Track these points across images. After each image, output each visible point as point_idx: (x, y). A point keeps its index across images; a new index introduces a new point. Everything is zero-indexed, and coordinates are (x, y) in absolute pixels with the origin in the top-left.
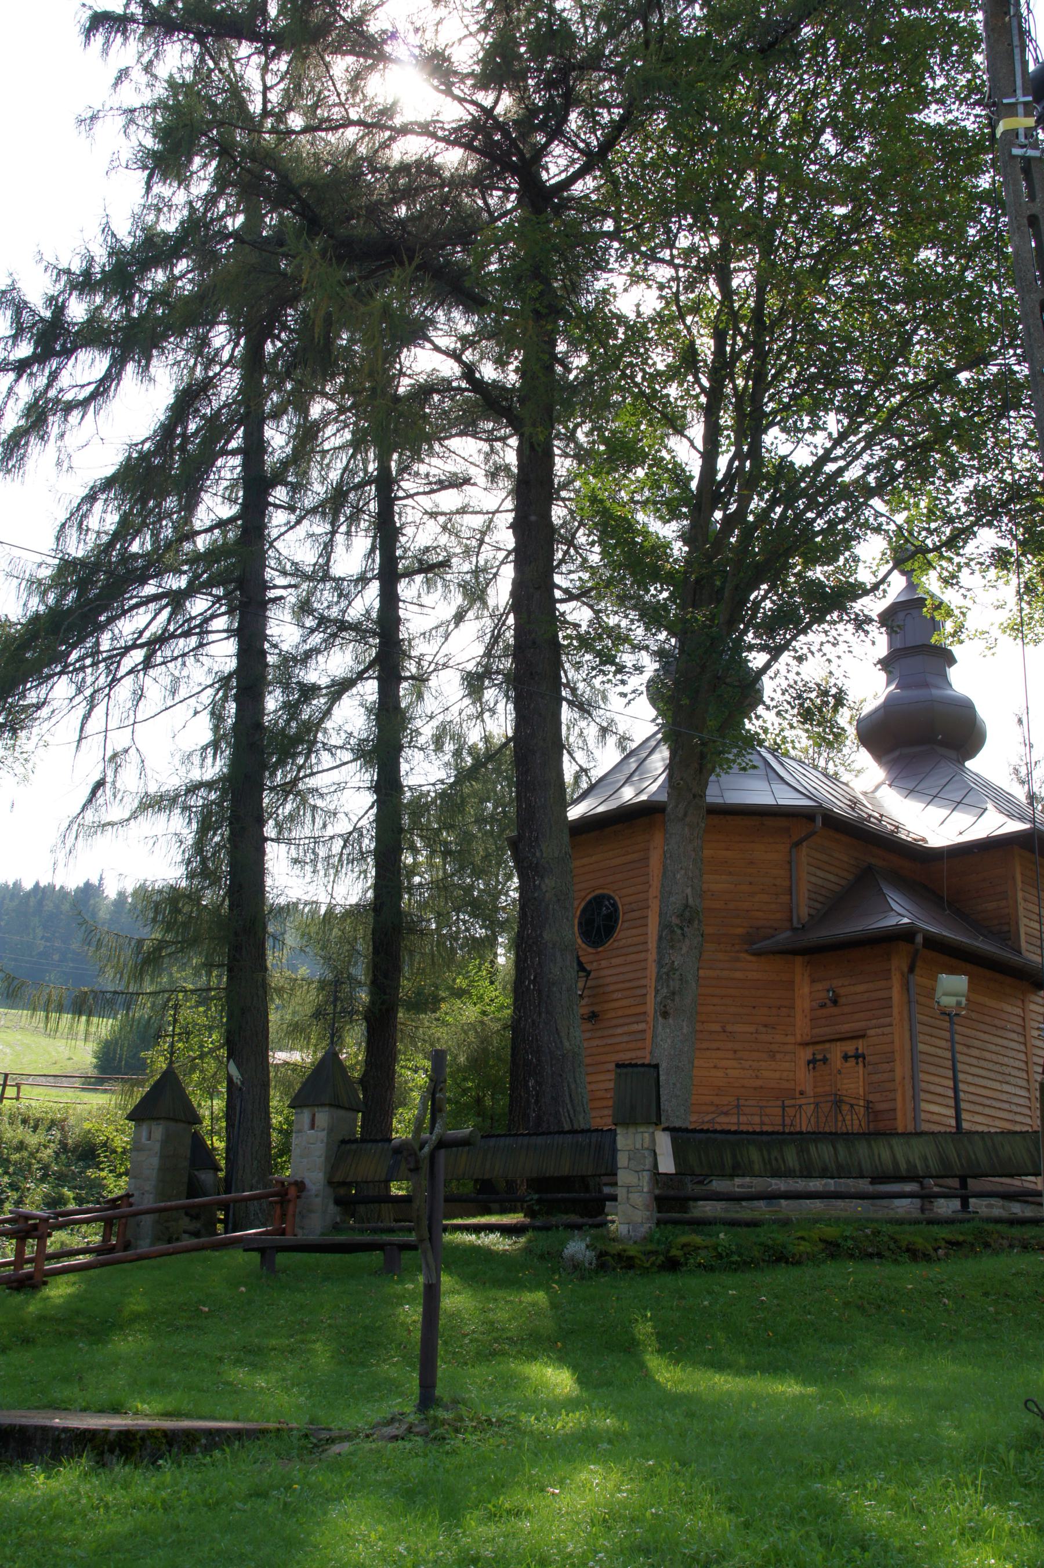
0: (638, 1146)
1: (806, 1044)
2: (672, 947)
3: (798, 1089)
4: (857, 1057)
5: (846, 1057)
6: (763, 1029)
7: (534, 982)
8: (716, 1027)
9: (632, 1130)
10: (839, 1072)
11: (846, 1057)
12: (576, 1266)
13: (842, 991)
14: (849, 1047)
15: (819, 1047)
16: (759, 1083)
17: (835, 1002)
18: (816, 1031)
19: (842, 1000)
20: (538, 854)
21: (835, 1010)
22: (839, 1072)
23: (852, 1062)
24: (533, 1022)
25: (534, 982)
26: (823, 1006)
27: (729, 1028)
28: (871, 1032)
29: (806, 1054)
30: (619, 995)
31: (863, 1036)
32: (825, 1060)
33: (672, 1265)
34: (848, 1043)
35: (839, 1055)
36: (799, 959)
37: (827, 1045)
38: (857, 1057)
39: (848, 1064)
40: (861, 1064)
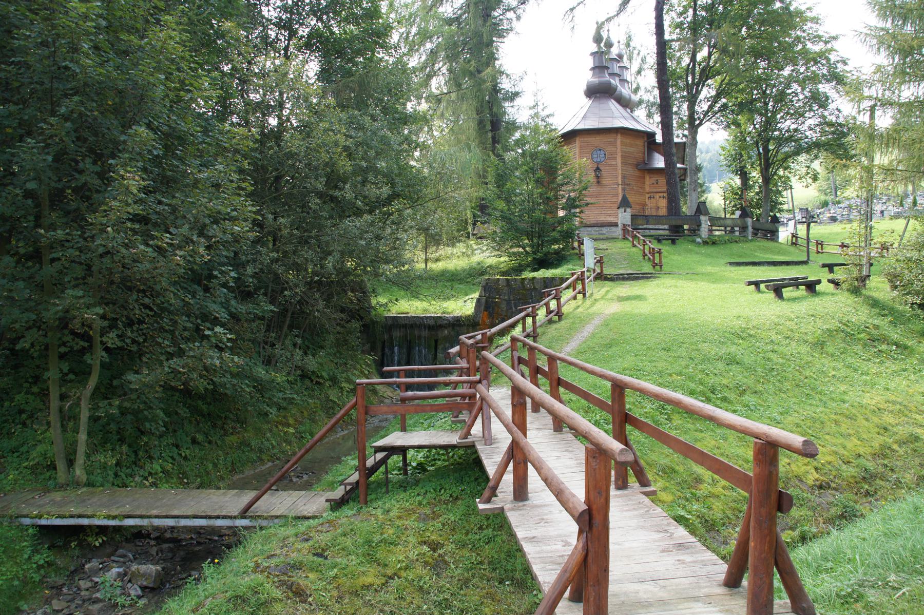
12: (699, 243)
29: (648, 195)
33: (714, 243)
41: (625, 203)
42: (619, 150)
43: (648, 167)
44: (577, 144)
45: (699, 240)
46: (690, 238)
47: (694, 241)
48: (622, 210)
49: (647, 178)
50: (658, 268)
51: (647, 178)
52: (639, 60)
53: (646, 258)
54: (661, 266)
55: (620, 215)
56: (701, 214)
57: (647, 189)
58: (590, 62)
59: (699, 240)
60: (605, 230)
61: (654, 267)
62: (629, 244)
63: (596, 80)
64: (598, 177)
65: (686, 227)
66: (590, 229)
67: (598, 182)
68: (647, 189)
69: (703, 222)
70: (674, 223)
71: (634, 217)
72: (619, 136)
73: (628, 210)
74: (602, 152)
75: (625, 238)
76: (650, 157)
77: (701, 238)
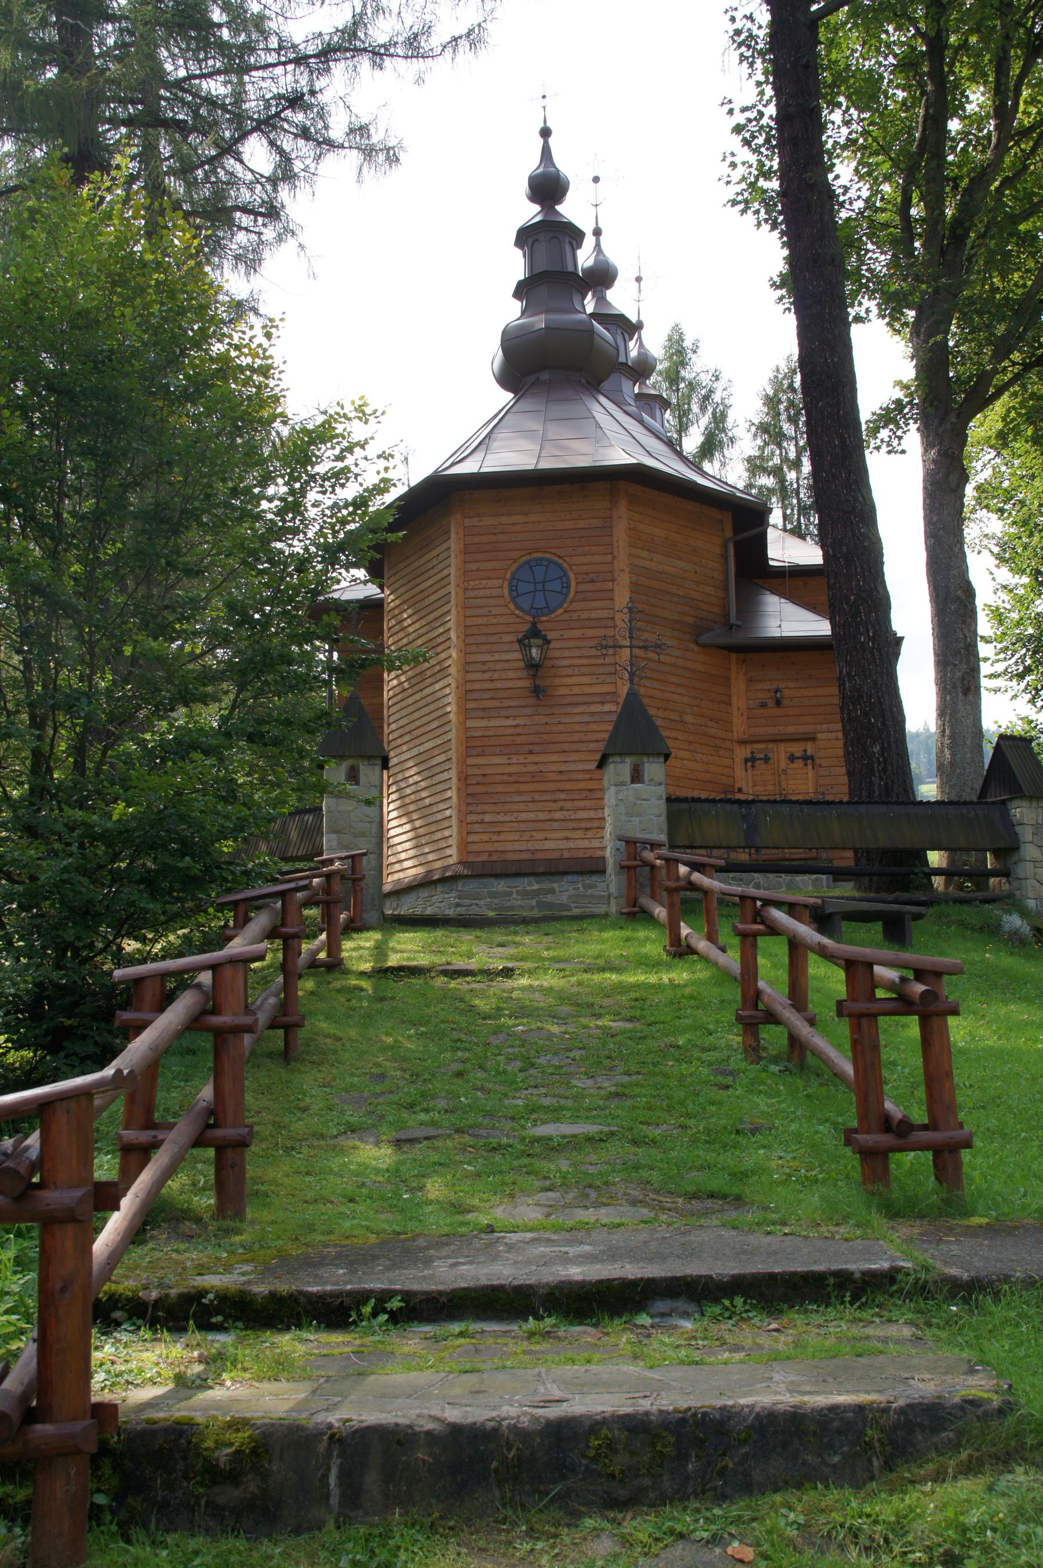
1: (743, 742)
2: (964, 622)
3: (737, 786)
4: (806, 758)
5: (792, 758)
6: (710, 723)
8: (675, 716)
9: (1035, 804)
11: (792, 758)
13: (786, 693)
14: (797, 749)
17: (778, 703)
18: (752, 730)
19: (785, 702)
21: (777, 711)
23: (799, 764)
24: (875, 682)
25: (873, 639)
26: (764, 705)
28: (819, 736)
29: (742, 753)
30: (569, 671)
31: (814, 739)
32: (766, 759)
34: (795, 744)
35: (783, 756)
36: (734, 656)
37: (771, 745)
38: (806, 758)
39: (795, 765)
40: (810, 767)
41: (634, 736)
42: (622, 562)
43: (738, 638)
44: (454, 543)
45: (1014, 921)
46: (966, 913)
47: (991, 931)
48: (620, 768)
49: (739, 685)
50: (911, 1165)
51: (739, 685)
52: (705, 421)
53: (772, 1037)
54: (947, 1157)
55: (610, 796)
56: (1017, 793)
57: (739, 726)
58: (515, 266)
59: (1014, 921)
60: (564, 891)
61: (875, 1162)
62: (652, 943)
63: (540, 322)
64: (533, 667)
65: (935, 858)
66: (501, 886)
67: (537, 691)
68: (739, 726)
69: (1026, 834)
70: (883, 837)
71: (678, 808)
72: (623, 508)
73: (654, 769)
75: (636, 914)
76: (749, 609)
77: (1024, 913)
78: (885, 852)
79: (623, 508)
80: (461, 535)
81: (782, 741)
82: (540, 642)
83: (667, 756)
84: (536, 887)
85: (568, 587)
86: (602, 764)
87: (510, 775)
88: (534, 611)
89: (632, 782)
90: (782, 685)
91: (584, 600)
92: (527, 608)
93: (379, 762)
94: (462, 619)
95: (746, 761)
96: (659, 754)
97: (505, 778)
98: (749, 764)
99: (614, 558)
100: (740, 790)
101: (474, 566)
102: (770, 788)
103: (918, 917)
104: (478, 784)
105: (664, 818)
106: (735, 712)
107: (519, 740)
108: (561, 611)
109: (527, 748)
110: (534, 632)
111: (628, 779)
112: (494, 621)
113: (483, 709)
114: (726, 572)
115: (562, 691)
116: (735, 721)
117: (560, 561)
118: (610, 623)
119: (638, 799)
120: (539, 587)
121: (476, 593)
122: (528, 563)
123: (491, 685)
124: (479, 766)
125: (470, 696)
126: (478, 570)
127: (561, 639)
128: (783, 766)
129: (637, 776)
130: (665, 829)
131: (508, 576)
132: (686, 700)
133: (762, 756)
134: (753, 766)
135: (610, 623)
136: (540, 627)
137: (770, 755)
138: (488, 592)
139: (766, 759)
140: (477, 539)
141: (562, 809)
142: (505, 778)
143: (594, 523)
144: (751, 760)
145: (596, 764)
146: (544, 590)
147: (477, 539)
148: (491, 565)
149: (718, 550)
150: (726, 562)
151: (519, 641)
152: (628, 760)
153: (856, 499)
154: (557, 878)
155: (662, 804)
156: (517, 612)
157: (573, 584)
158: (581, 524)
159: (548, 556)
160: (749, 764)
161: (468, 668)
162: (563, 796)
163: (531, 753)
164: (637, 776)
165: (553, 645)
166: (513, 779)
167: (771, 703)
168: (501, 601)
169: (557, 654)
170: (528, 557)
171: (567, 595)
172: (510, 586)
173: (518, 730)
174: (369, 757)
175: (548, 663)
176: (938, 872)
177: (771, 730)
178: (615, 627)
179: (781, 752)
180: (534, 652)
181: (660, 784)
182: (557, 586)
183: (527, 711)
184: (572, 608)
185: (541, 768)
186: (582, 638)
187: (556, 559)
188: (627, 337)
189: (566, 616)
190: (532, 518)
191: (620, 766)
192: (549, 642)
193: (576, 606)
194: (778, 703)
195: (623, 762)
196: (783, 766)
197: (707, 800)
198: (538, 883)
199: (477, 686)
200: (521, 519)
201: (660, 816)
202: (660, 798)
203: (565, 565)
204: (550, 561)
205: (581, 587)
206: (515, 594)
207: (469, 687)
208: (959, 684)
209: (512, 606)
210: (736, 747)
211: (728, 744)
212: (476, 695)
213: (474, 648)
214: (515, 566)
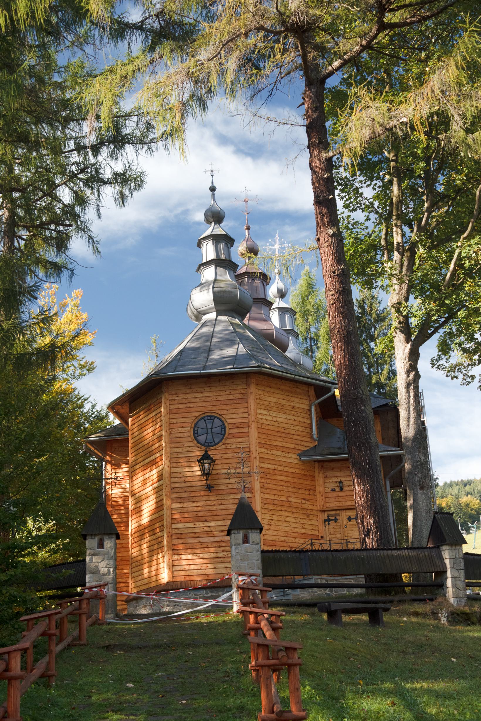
0: (457, 557)
1: (323, 511)
6: (304, 501)
7: (369, 464)
9: (454, 547)
10: (346, 526)
11: (350, 519)
13: (345, 483)
15: (333, 512)
16: (303, 531)
17: (341, 489)
18: (328, 505)
19: (345, 489)
20: (361, 392)
21: (341, 494)
22: (346, 526)
25: (369, 464)
26: (333, 490)
27: (290, 499)
32: (336, 520)
37: (338, 512)
39: (351, 523)
48: (238, 536)
49: (320, 478)
67: (209, 487)
68: (320, 503)
73: (253, 536)
74: (217, 422)
78: (379, 575)
79: (253, 388)
80: (168, 404)
81: (344, 510)
82: (209, 461)
83: (261, 530)
84: (210, 594)
85: (225, 431)
86: (229, 533)
87: (195, 533)
88: (206, 444)
89: (244, 543)
90: (343, 479)
91: (233, 438)
92: (203, 442)
93: (114, 536)
94: (168, 449)
95: (325, 521)
96: (256, 529)
97: (193, 535)
98: (327, 523)
99: (249, 415)
100: (322, 537)
101: (175, 421)
102: (338, 536)
103: (386, 610)
104: (178, 538)
105: (260, 561)
106: (318, 495)
107: (200, 514)
108: (221, 444)
109: (204, 518)
110: (206, 456)
111: (241, 542)
112: (186, 450)
113: (181, 498)
114: (311, 419)
115: (223, 487)
116: (318, 499)
117: (220, 417)
118: (248, 450)
119: (247, 552)
120: (209, 431)
121: (176, 435)
122: (203, 418)
123: (183, 485)
124: (178, 529)
125: (173, 491)
126: (177, 423)
127: (221, 459)
128: (345, 523)
129: (246, 540)
130: (261, 567)
131: (193, 425)
132: (290, 489)
133: (333, 518)
134: (329, 524)
135: (248, 450)
136: (210, 453)
137: (338, 518)
138: (182, 435)
139: (336, 520)
140: (176, 406)
141: (223, 551)
142: (193, 535)
143: (237, 396)
144: (328, 520)
145: (226, 533)
146: (212, 433)
147: (176, 406)
148: (182, 420)
149: (306, 407)
150: (311, 414)
151: (199, 461)
152: (241, 532)
153: (358, 392)
154: (221, 589)
155: (259, 553)
156: (198, 445)
157: (227, 429)
158: (231, 397)
159: (213, 414)
160: (327, 523)
161: (172, 476)
162: (224, 544)
163: (206, 521)
164: (246, 540)
165: (217, 462)
166: (197, 535)
167: (337, 489)
168: (190, 439)
169: (220, 467)
170: (203, 415)
171: (224, 435)
172: (194, 431)
173: (199, 509)
174: (109, 534)
175: (214, 472)
176: (408, 585)
177: (338, 504)
178: (250, 452)
179: (344, 515)
180: (207, 466)
181: (258, 544)
182: (218, 430)
183: (204, 498)
184: (227, 442)
185: (212, 529)
186: (233, 458)
187: (218, 416)
188: (265, 283)
189: (224, 447)
190: (206, 394)
191: (237, 535)
192: (214, 461)
193: (228, 441)
194: (341, 489)
195: (238, 533)
196: (345, 523)
197: (283, 551)
198: (211, 592)
199: (177, 485)
200: (200, 395)
201: (257, 560)
202: (257, 551)
203: (223, 419)
204: (215, 417)
205: (232, 431)
206: (196, 435)
207: (173, 486)
208: (418, 484)
209: (195, 442)
210: (319, 514)
211: (315, 512)
212: (176, 490)
213: (175, 465)
214: (196, 420)
